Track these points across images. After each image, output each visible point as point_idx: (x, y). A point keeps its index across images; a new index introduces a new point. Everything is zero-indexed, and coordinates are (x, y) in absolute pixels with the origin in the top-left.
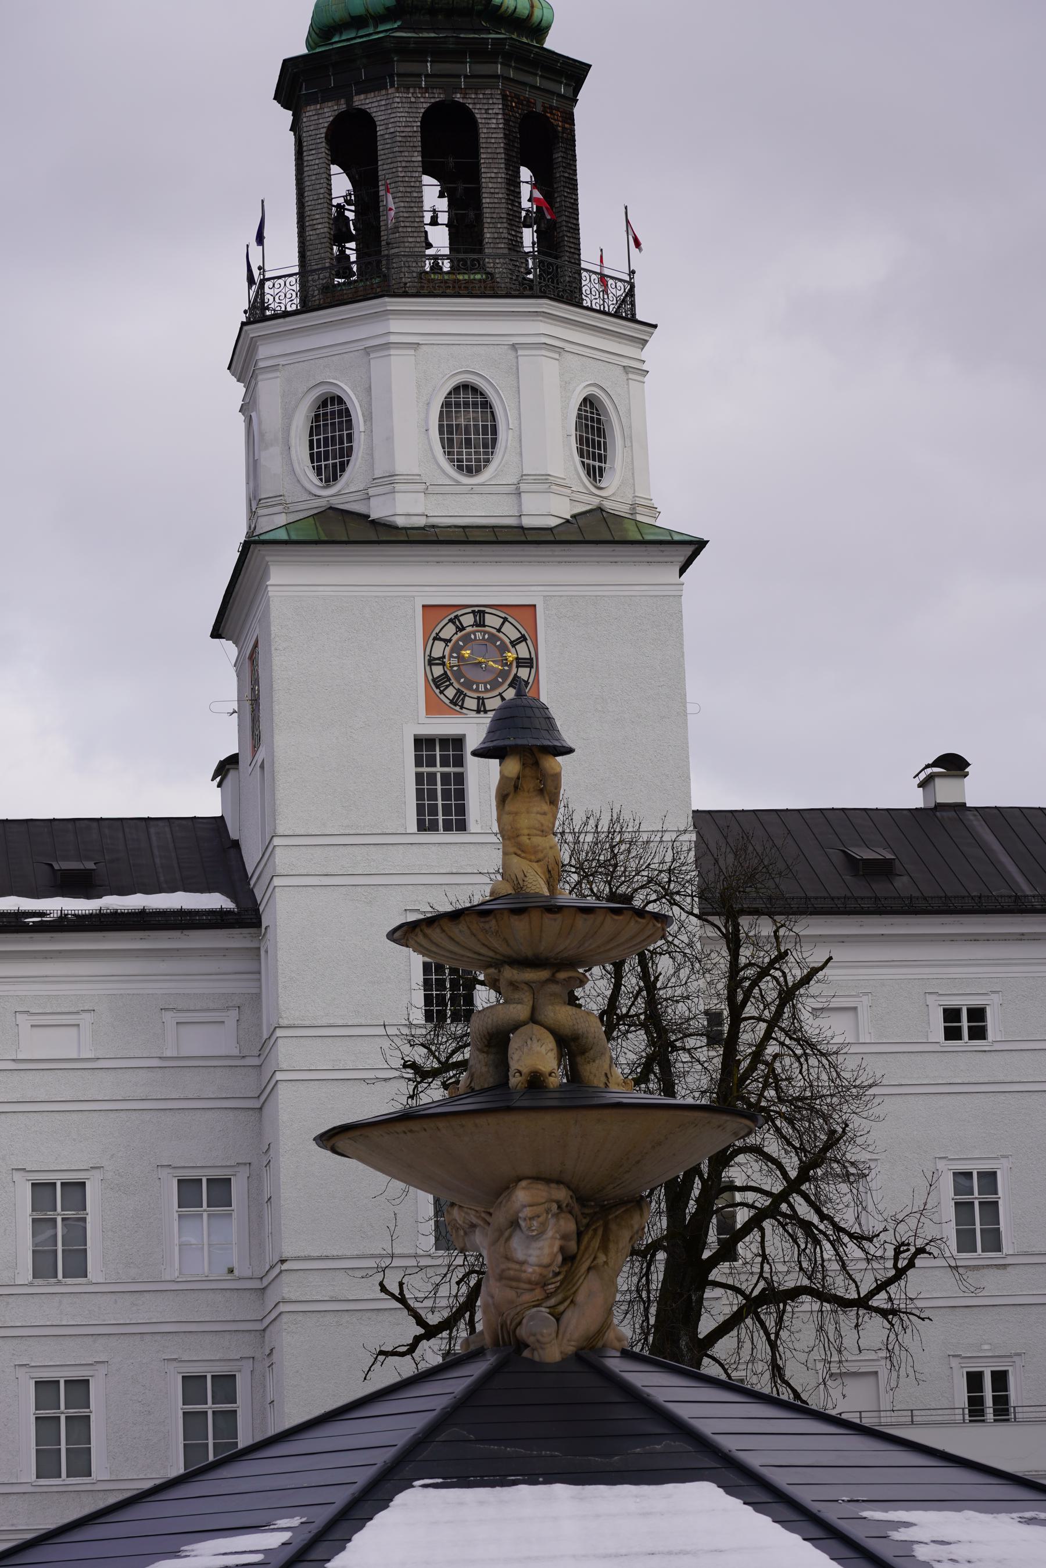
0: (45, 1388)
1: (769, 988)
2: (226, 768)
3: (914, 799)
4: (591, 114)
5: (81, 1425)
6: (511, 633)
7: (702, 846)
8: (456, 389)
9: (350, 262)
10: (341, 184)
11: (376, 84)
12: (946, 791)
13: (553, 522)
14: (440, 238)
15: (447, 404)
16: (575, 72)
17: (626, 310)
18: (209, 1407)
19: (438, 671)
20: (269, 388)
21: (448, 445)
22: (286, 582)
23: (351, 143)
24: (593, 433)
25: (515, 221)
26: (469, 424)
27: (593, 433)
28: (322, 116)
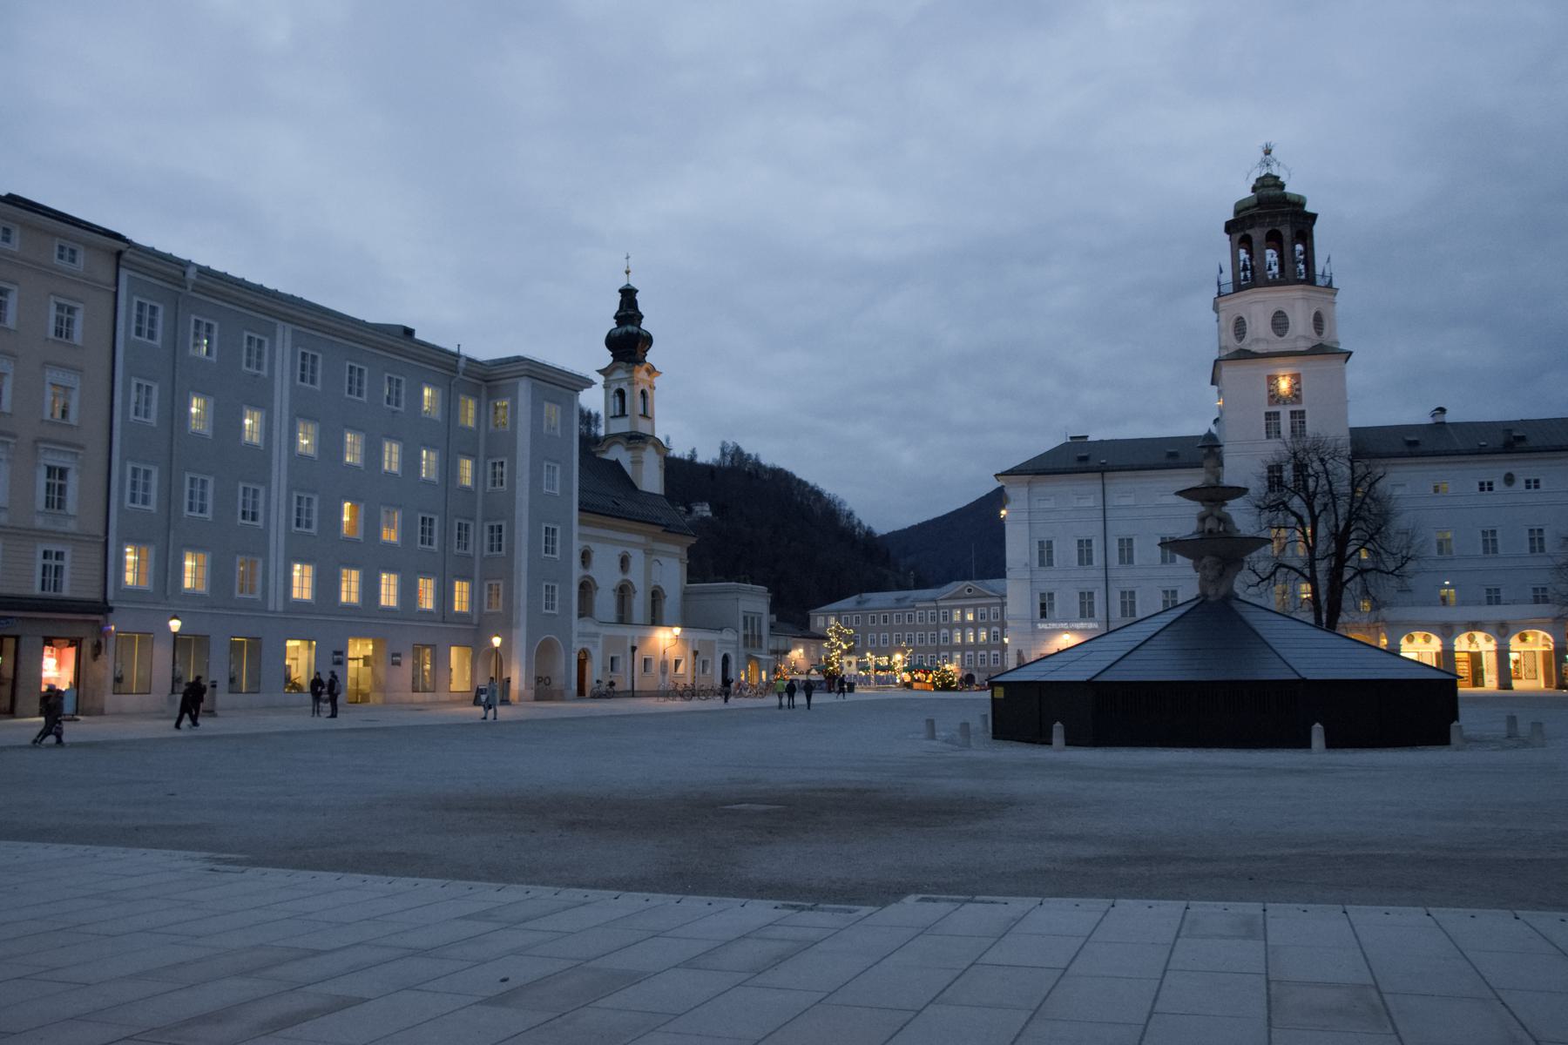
1: (1365, 484)
2: (1216, 421)
3: (1430, 421)
4: (1318, 229)
7: (1352, 442)
9: (1248, 279)
10: (1243, 254)
11: (1251, 227)
12: (1439, 419)
14: (1275, 269)
16: (1313, 217)
17: (1329, 285)
20: (1222, 315)
22: (1227, 371)
23: (1246, 242)
24: (1318, 321)
25: (1296, 263)
26: (1280, 322)
27: (1318, 321)
28: (1238, 236)
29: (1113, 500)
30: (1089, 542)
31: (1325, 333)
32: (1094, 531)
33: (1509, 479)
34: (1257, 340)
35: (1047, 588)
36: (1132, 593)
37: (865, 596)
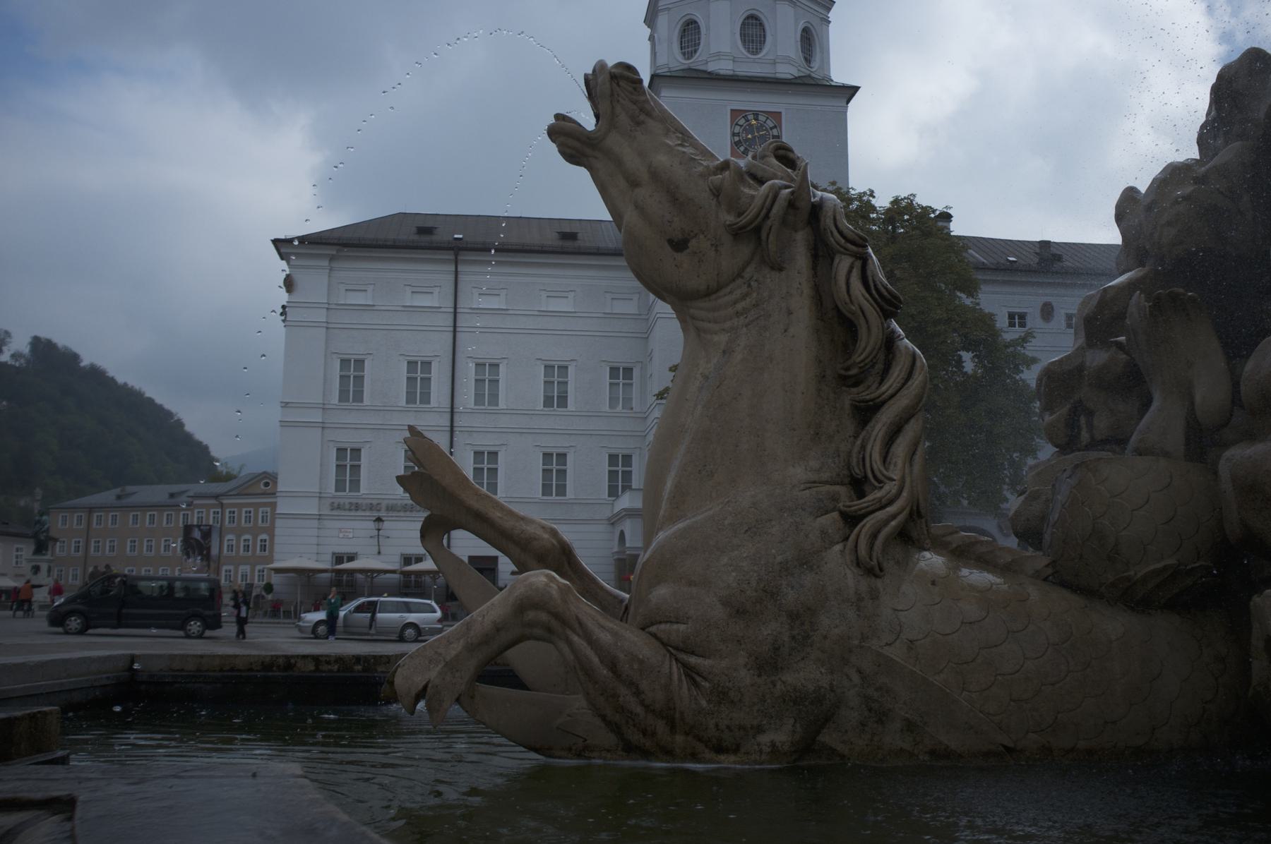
0: (547, 456)
5: (562, 473)
6: (770, 124)
8: (748, 18)
13: (789, 77)
15: (743, 24)
18: (620, 468)
19: (737, 139)
21: (744, 42)
29: (472, 299)
30: (427, 365)
31: (816, 65)
32: (435, 346)
33: (1047, 312)
34: (718, 56)
35: (349, 439)
36: (493, 455)
37: (129, 489)
